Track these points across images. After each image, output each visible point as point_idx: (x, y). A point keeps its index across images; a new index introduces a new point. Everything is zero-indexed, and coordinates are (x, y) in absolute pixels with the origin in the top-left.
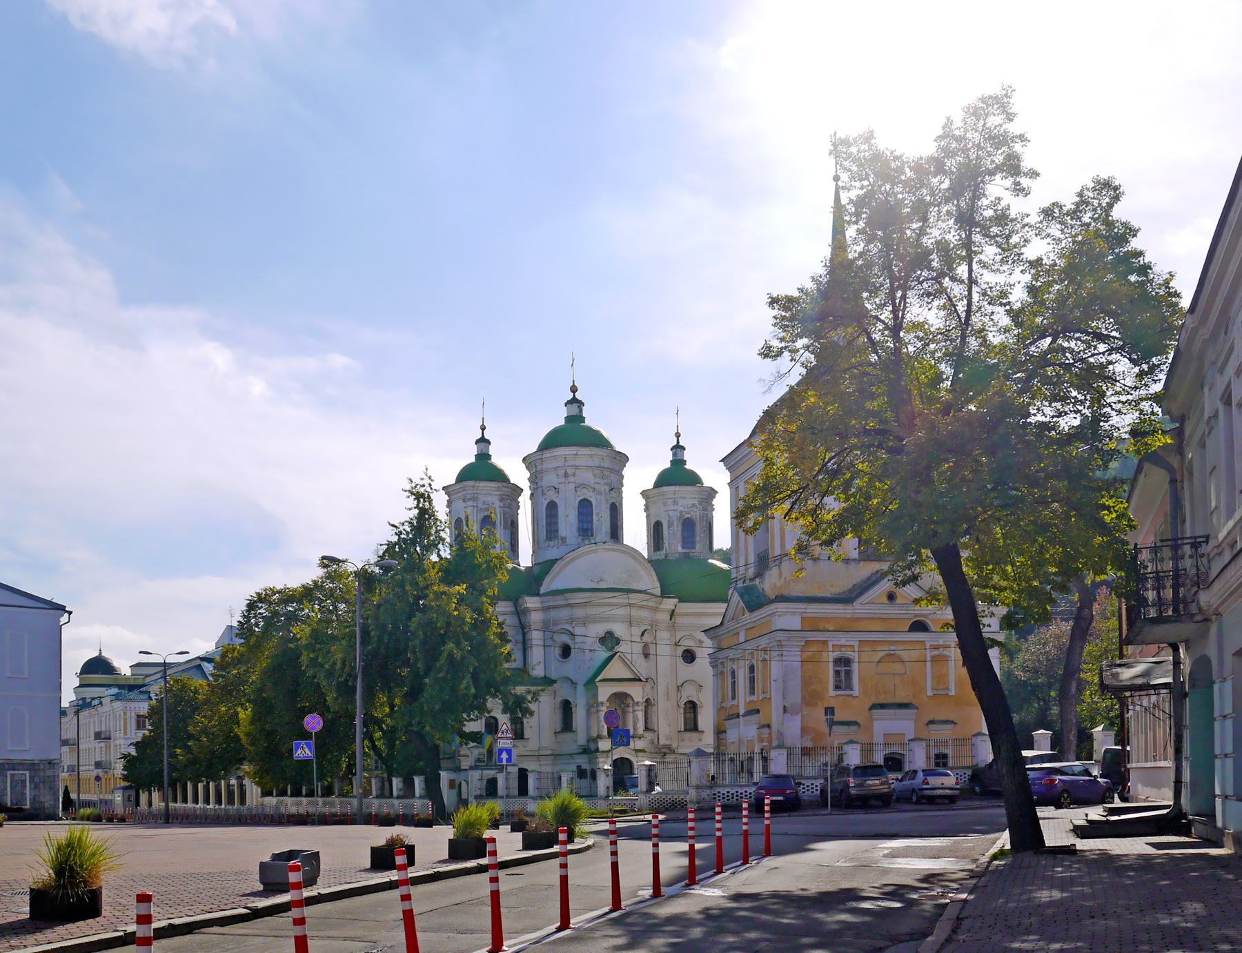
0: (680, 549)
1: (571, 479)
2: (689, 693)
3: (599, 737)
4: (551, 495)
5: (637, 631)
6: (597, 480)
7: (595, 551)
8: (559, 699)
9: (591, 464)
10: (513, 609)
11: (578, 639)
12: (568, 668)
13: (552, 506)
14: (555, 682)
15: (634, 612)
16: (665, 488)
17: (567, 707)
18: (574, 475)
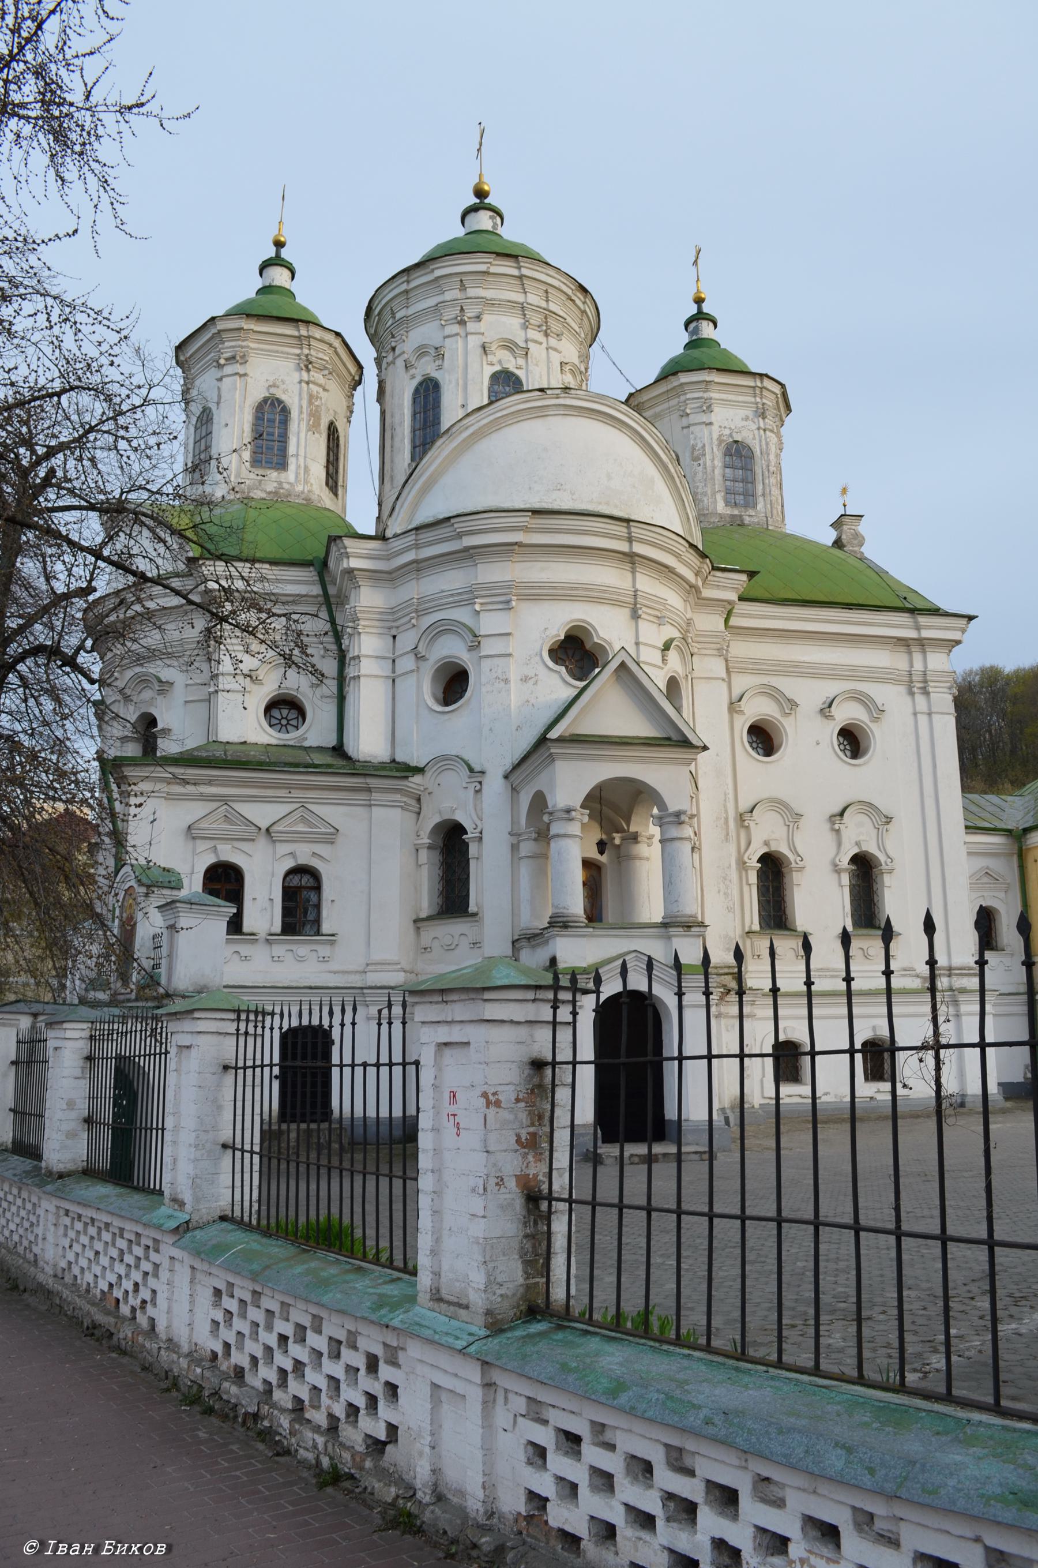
0: (721, 507)
1: (471, 326)
2: (768, 833)
3: (560, 923)
4: (427, 367)
5: (653, 635)
6: (532, 334)
7: (541, 412)
8: (431, 819)
9: (520, 298)
10: (316, 590)
11: (488, 647)
12: (456, 731)
13: (428, 394)
14: (419, 770)
15: (647, 584)
16: (684, 378)
17: (452, 844)
18: (478, 318)
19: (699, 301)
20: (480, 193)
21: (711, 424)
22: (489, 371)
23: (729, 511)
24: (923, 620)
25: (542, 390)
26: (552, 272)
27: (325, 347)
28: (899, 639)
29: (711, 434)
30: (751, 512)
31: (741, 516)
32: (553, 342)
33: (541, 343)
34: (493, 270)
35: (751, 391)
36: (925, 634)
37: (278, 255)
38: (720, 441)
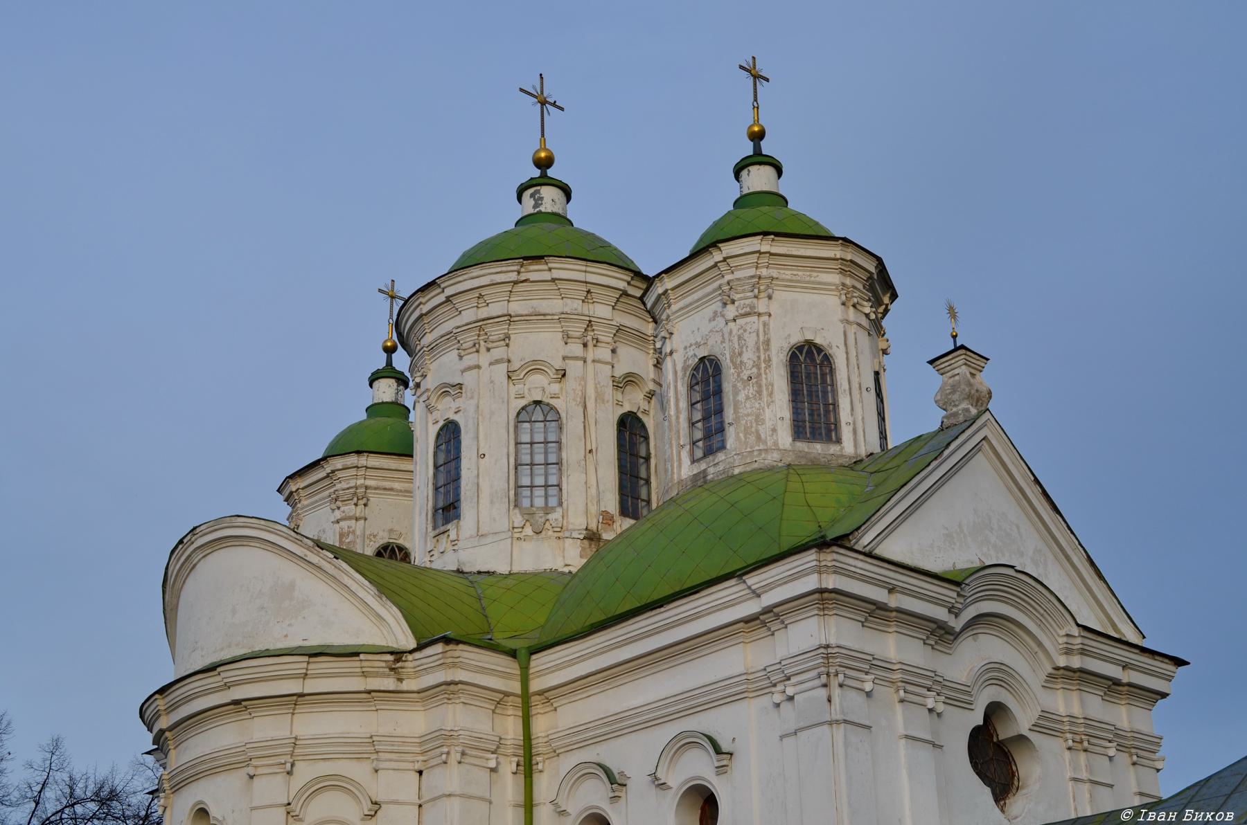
19: (757, 137)
20: (544, 164)
21: (671, 353)
22: (434, 430)
23: (696, 469)
24: (754, 580)
25: (181, 542)
26: (475, 272)
27: (353, 472)
28: (748, 620)
29: (675, 365)
30: (721, 456)
31: (705, 471)
33: (478, 367)
34: (425, 309)
35: (715, 272)
36: (769, 599)
37: (389, 362)
38: (685, 369)
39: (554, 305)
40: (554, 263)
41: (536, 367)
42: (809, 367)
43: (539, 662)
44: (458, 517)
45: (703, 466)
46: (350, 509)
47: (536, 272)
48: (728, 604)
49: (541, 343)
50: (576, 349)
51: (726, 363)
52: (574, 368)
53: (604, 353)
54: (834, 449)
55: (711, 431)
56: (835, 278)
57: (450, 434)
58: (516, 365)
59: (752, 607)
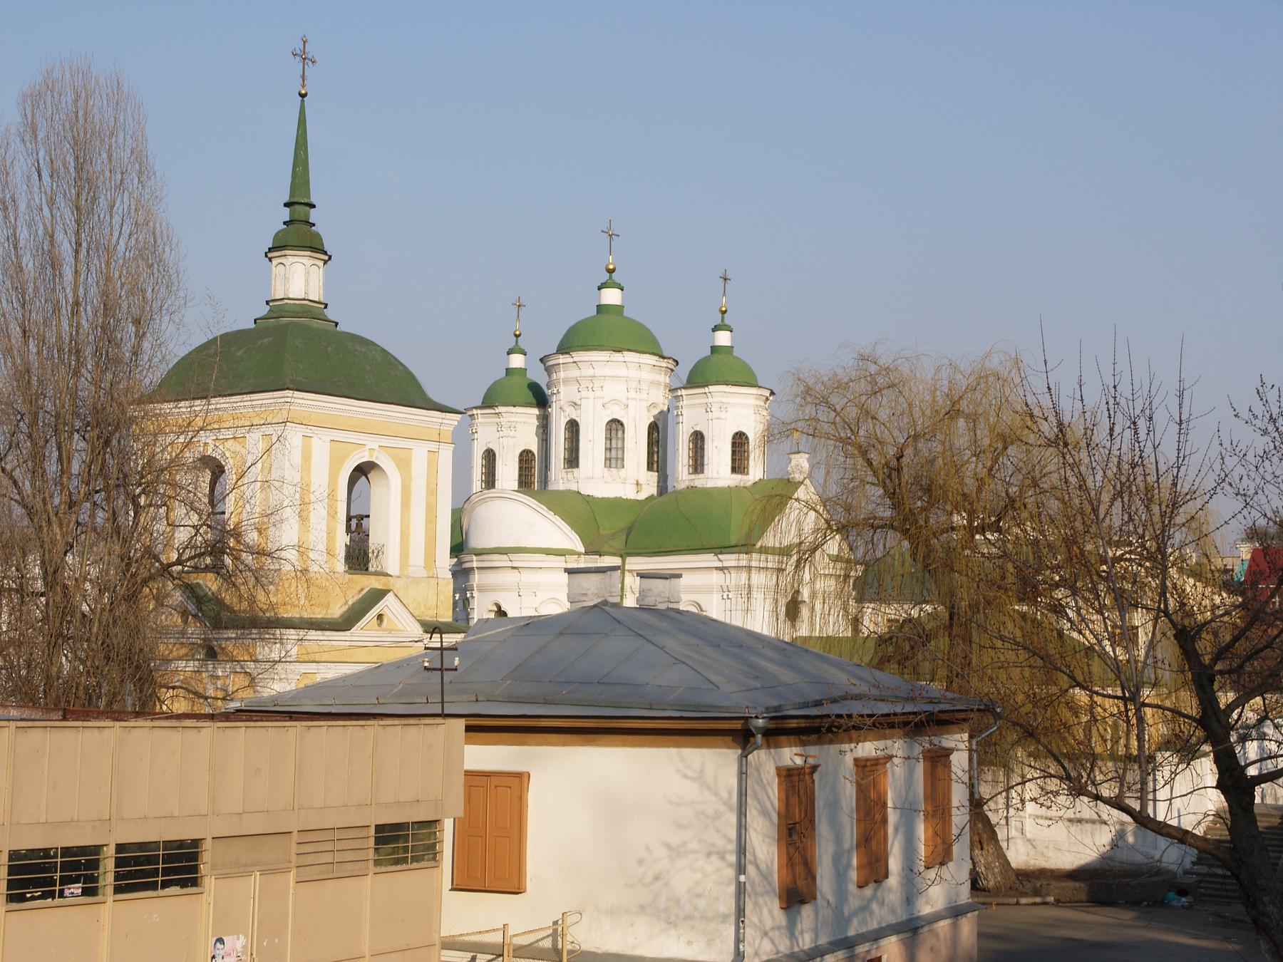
30: (701, 476)
32: (598, 393)
39: (622, 372)
40: (626, 353)
41: (615, 401)
42: (739, 441)
43: (629, 559)
44: (577, 466)
45: (693, 477)
46: (506, 432)
47: (618, 356)
48: (708, 560)
49: (615, 390)
50: (632, 394)
51: (705, 434)
52: (631, 403)
53: (644, 395)
54: (744, 477)
55: (698, 464)
56: (752, 401)
57: (573, 427)
58: (606, 400)
59: (720, 564)
